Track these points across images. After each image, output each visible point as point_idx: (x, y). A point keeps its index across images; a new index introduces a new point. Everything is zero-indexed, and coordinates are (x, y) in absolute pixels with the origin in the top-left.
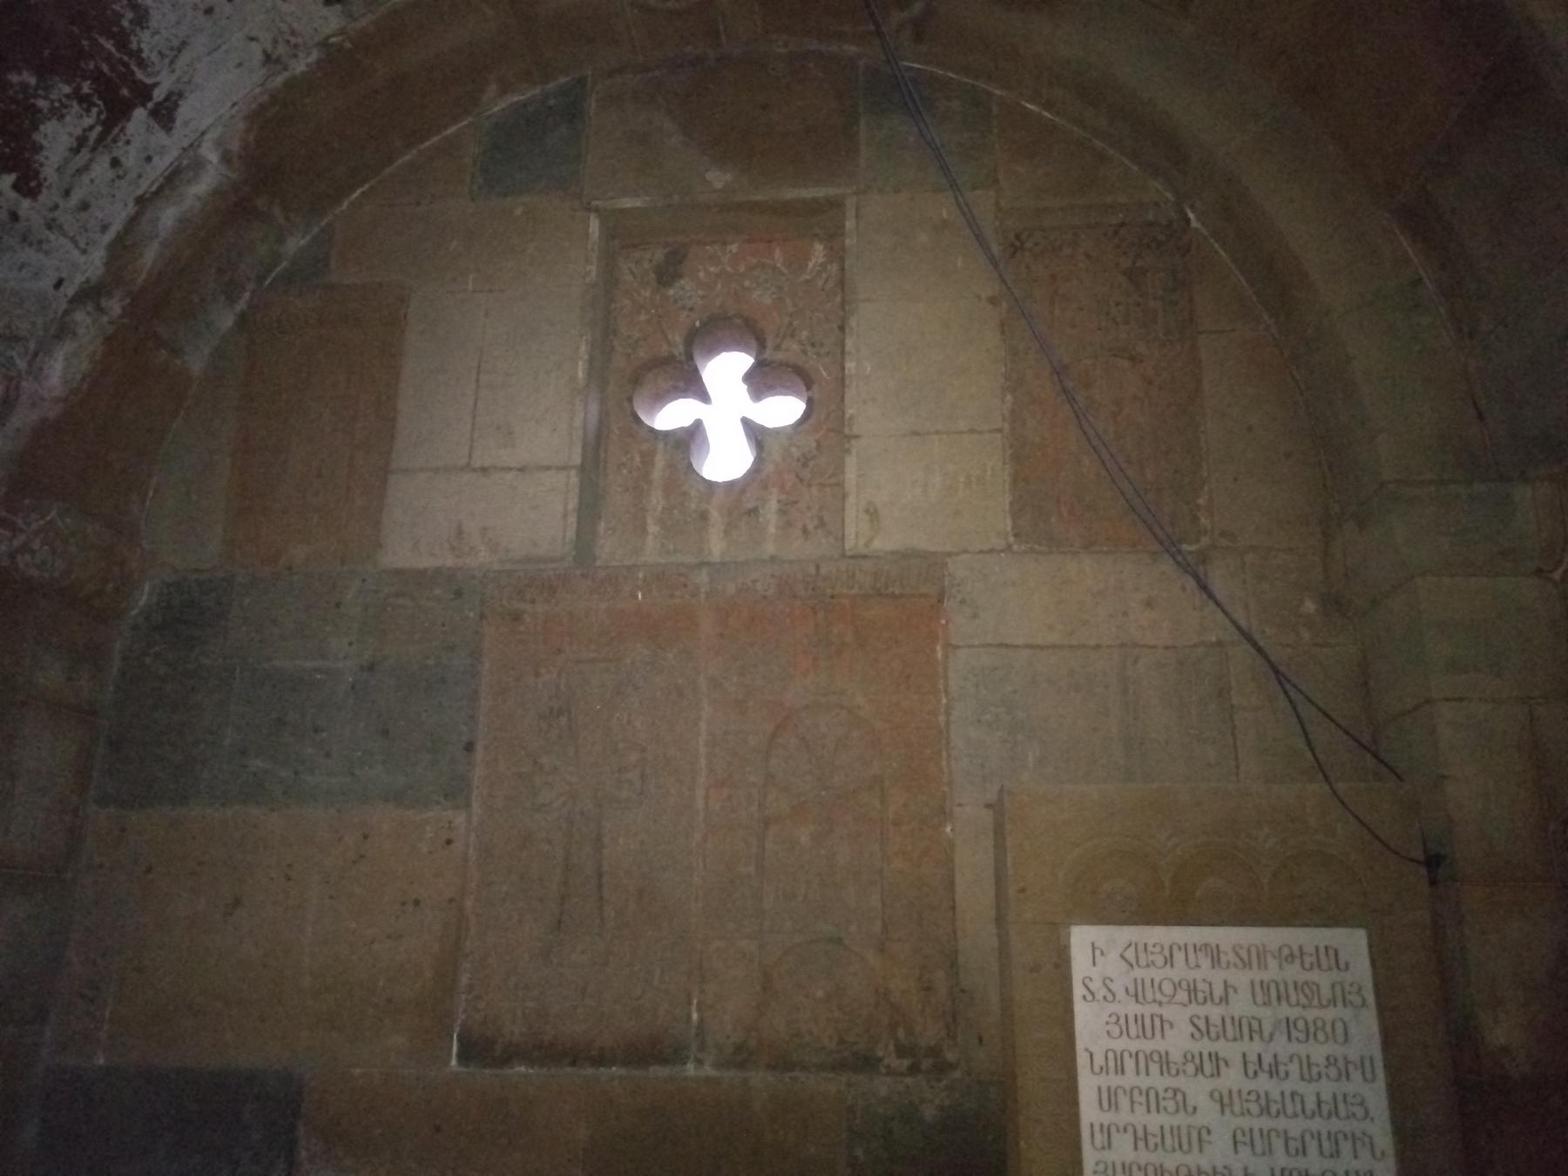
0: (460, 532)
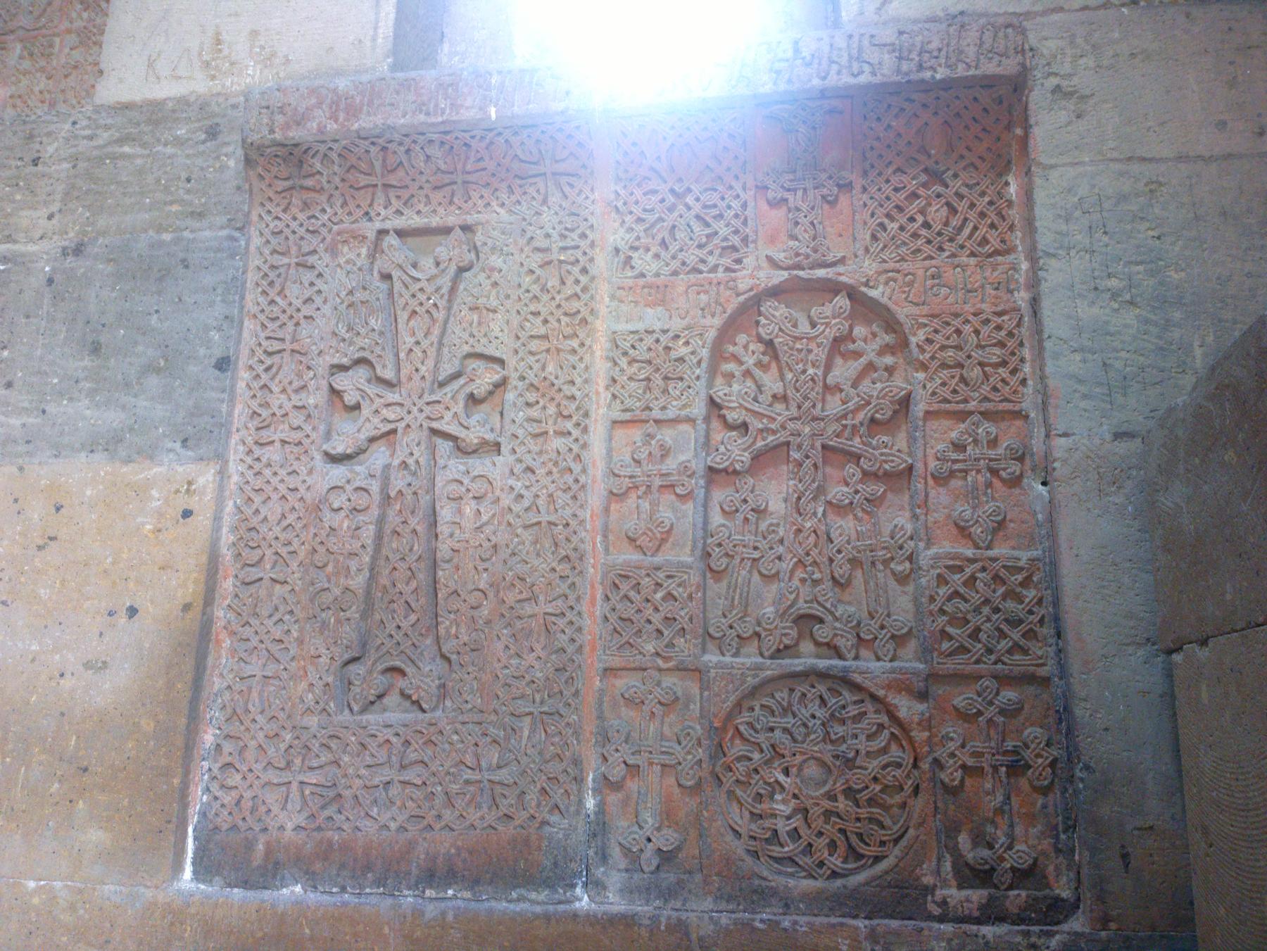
0: (219, 42)
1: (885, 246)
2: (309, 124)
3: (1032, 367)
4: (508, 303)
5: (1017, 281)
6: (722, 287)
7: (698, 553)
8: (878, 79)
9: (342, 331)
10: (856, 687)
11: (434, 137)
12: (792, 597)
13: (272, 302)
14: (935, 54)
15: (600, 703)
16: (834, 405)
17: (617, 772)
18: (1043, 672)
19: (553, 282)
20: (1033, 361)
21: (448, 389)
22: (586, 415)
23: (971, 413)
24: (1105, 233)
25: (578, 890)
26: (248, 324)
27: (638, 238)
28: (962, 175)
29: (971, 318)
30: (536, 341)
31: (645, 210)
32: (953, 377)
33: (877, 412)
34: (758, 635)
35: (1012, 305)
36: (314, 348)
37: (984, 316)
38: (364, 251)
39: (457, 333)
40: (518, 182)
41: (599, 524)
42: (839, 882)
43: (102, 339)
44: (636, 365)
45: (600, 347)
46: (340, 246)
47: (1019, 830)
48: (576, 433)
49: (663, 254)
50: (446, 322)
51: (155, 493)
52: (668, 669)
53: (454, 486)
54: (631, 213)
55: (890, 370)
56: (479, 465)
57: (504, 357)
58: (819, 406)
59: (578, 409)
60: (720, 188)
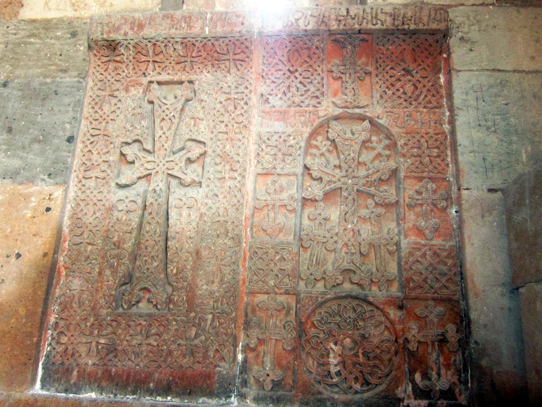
1: (386, 101)
2: (120, 31)
3: (451, 159)
4: (209, 117)
5: (444, 120)
6: (311, 114)
7: (297, 238)
8: (385, 27)
9: (128, 126)
10: (371, 304)
11: (178, 40)
12: (342, 260)
13: (96, 112)
14: (410, 18)
15: (247, 308)
16: (362, 172)
17: (253, 343)
18: (456, 298)
19: (231, 108)
20: (451, 156)
21: (177, 155)
22: (245, 170)
23: (425, 178)
24: (484, 101)
25: (232, 398)
26: (83, 122)
27: (272, 90)
28: (420, 72)
29: (424, 135)
30: (222, 134)
31: (276, 78)
32: (416, 161)
33: (382, 175)
34: (324, 278)
35: (442, 131)
36: (114, 133)
37: (430, 135)
38: (141, 91)
39: (184, 129)
40: (216, 62)
41: (249, 223)
42: (358, 396)
43: (13, 126)
44: (269, 148)
45: (253, 138)
46: (130, 88)
47: (443, 371)
48: (239, 178)
49: (284, 98)
50: (178, 125)
51: (33, 199)
52: (281, 294)
53: (178, 202)
54: (269, 79)
55: (388, 157)
56: (192, 192)
57: (206, 141)
58: (356, 171)
59: (240, 167)
60: (311, 70)
